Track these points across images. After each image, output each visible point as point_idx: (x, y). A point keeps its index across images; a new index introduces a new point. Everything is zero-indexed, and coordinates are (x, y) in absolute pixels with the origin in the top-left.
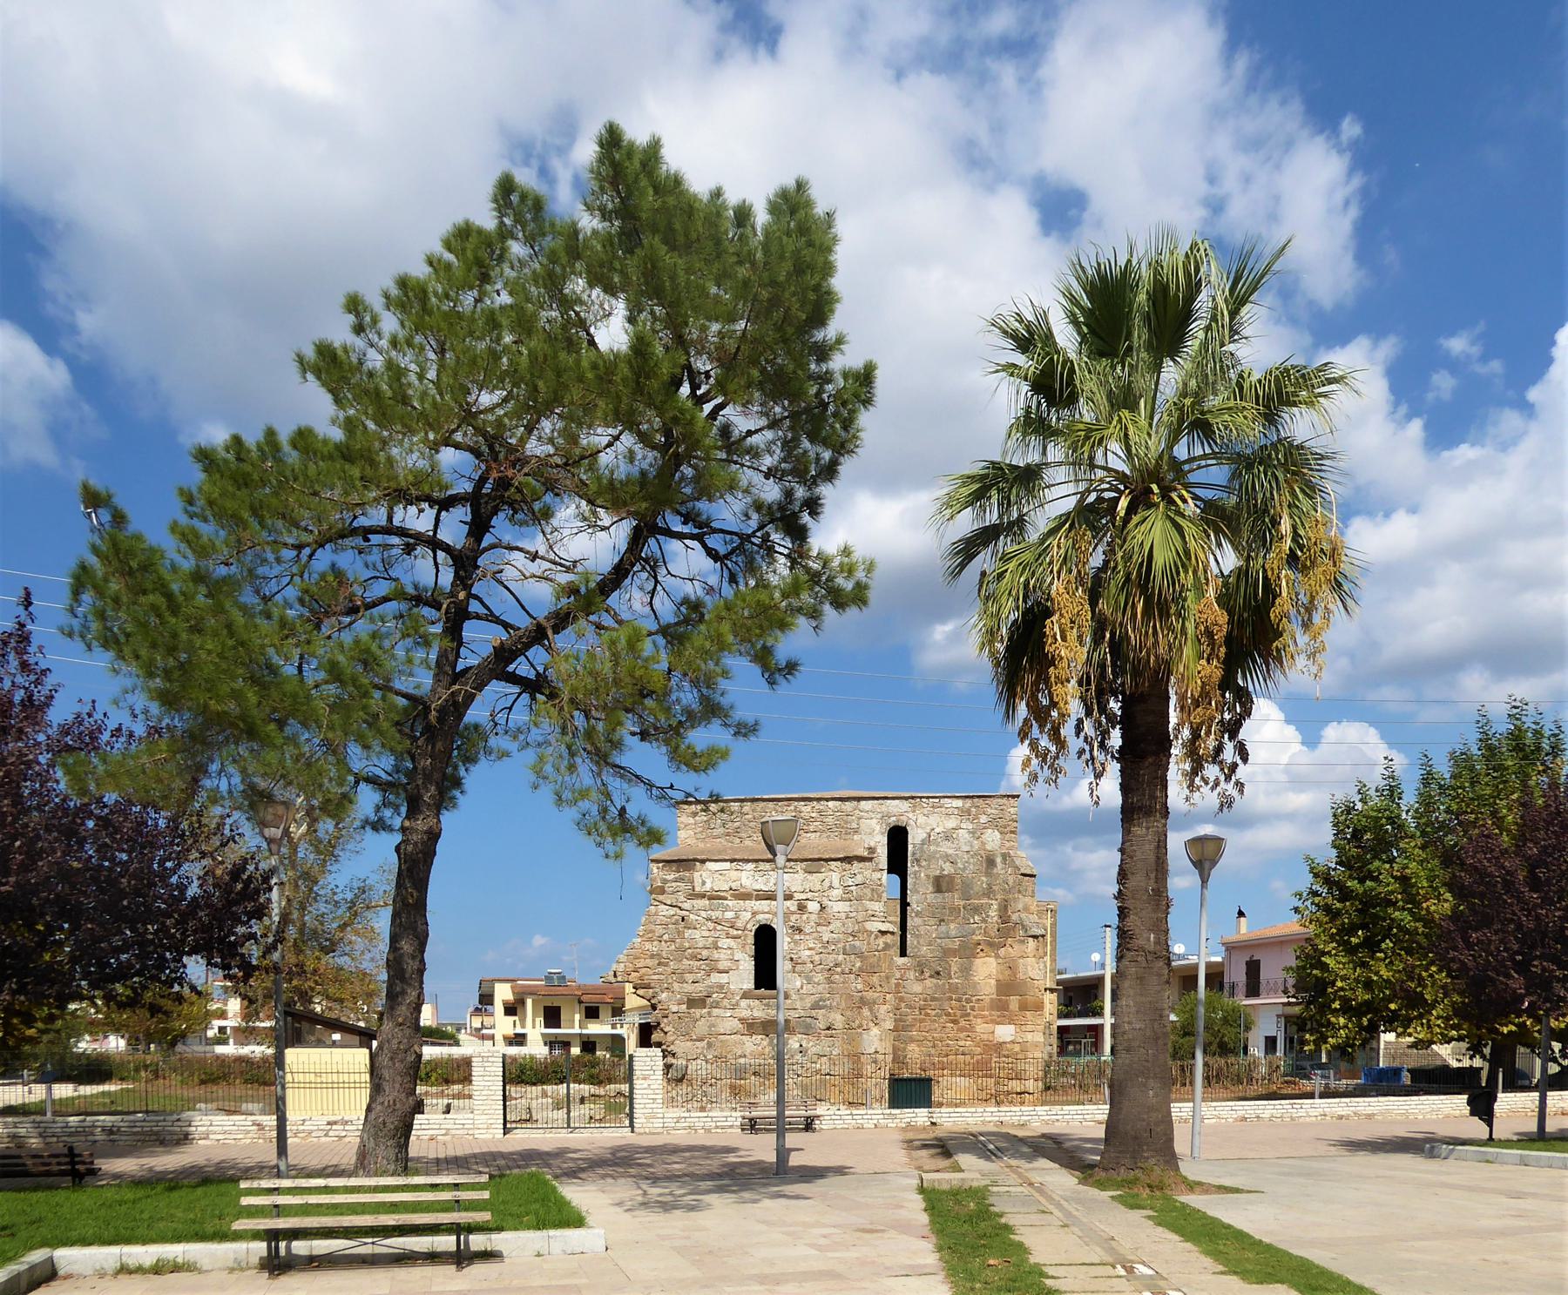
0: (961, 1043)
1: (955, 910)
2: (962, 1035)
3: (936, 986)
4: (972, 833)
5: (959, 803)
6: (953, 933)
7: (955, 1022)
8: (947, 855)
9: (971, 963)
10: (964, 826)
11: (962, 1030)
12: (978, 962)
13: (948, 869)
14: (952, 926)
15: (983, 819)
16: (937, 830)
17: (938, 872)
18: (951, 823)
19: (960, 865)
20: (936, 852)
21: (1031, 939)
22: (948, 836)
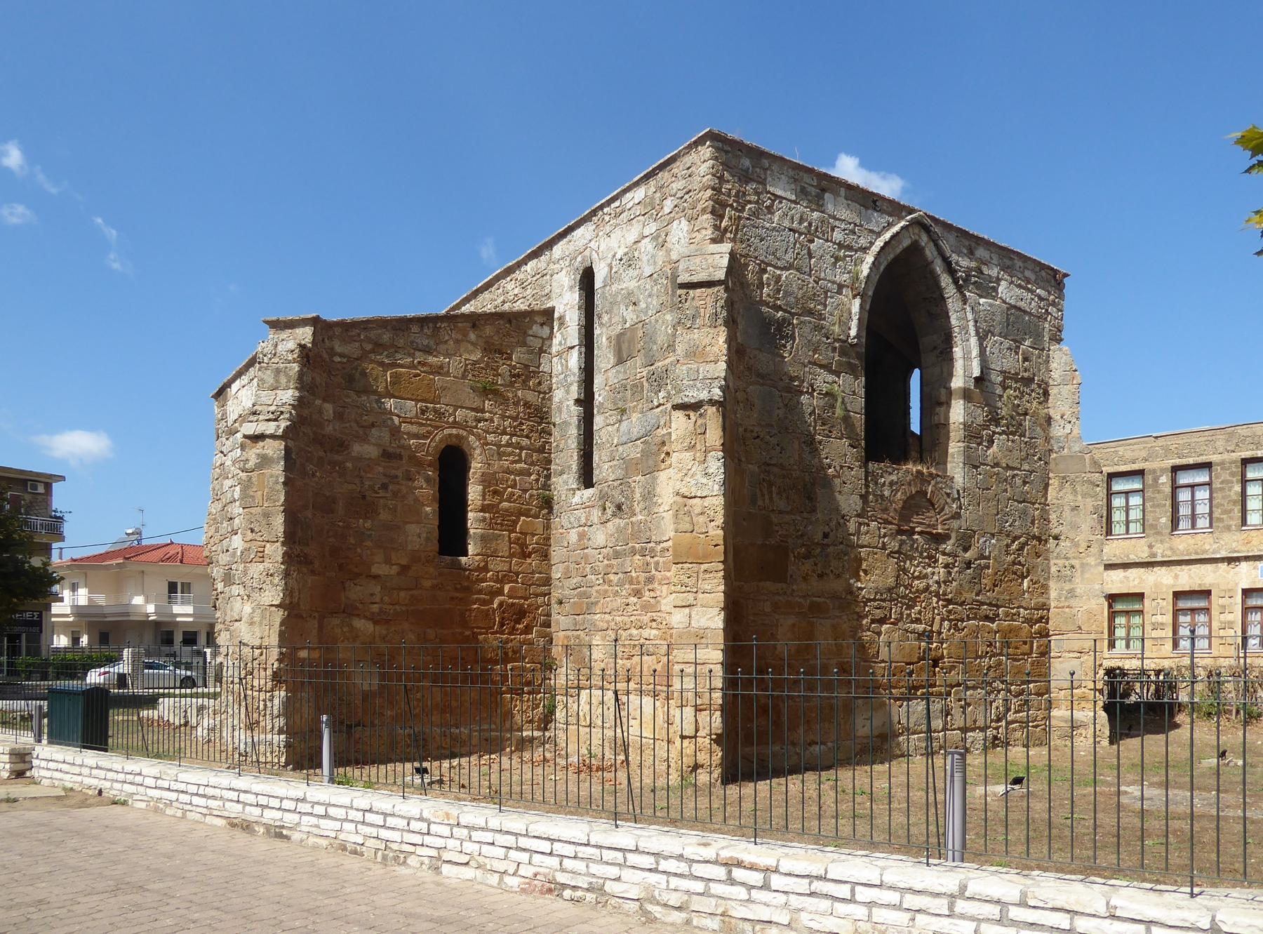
0: (646, 633)
1: (637, 388)
2: (646, 619)
3: (620, 530)
4: (655, 238)
5: (639, 194)
6: (635, 432)
7: (637, 593)
8: (630, 294)
9: (655, 479)
10: (646, 232)
11: (646, 608)
12: (662, 476)
13: (630, 316)
14: (635, 417)
15: (669, 205)
16: (618, 256)
17: (618, 329)
18: (632, 235)
19: (643, 305)
20: (618, 293)
21: (679, 414)
22: (629, 261)
